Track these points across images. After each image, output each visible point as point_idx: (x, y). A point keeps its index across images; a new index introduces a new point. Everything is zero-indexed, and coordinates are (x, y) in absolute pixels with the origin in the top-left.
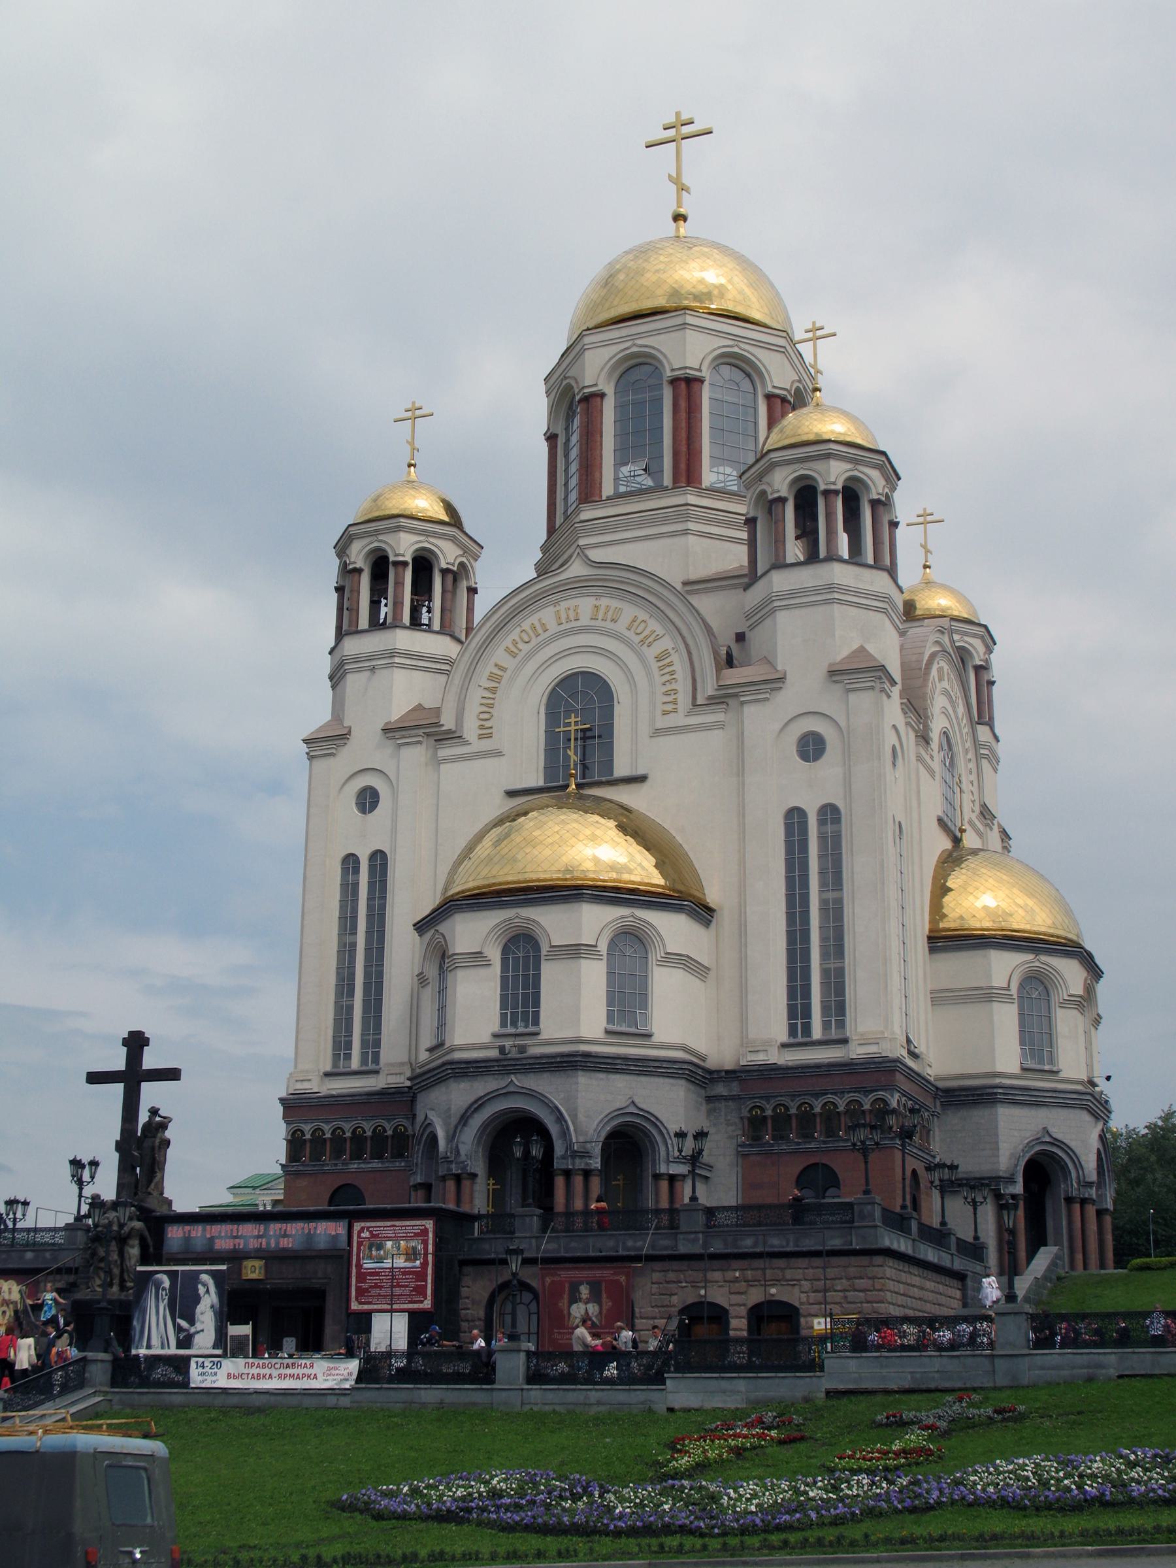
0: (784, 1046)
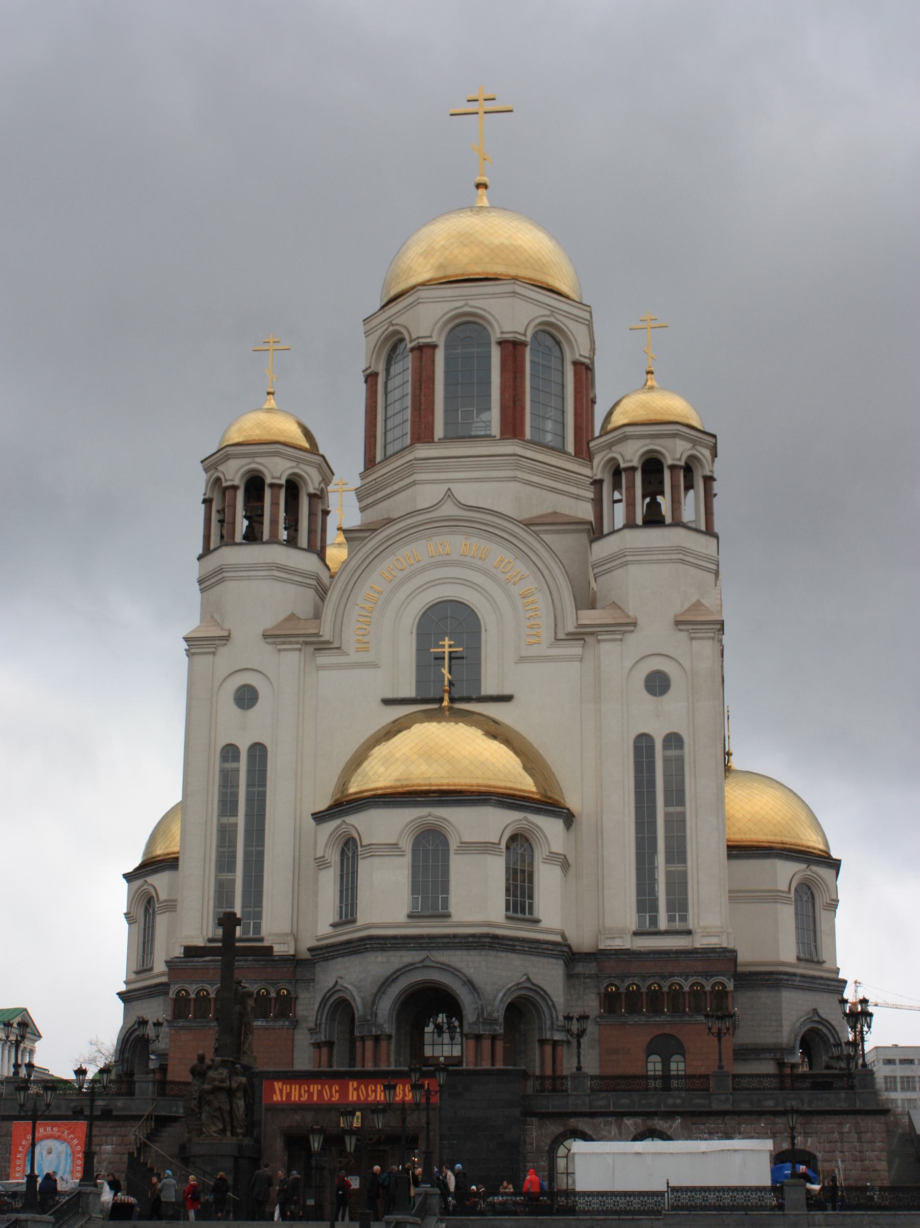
0: (635, 934)
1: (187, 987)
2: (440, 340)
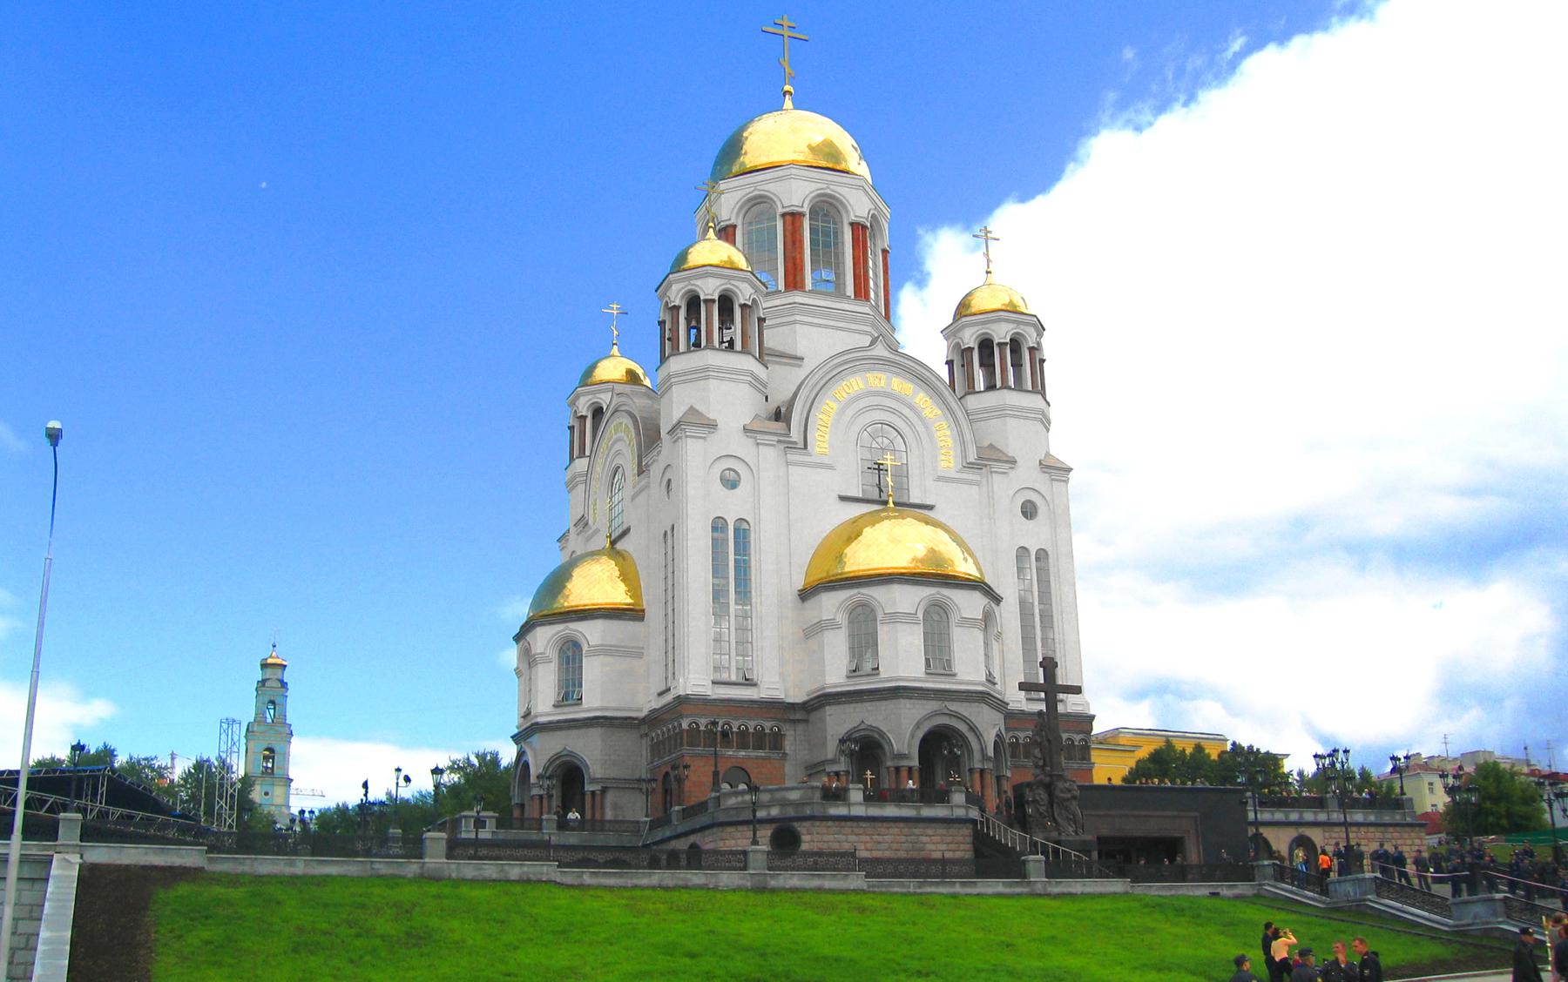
2: (806, 209)
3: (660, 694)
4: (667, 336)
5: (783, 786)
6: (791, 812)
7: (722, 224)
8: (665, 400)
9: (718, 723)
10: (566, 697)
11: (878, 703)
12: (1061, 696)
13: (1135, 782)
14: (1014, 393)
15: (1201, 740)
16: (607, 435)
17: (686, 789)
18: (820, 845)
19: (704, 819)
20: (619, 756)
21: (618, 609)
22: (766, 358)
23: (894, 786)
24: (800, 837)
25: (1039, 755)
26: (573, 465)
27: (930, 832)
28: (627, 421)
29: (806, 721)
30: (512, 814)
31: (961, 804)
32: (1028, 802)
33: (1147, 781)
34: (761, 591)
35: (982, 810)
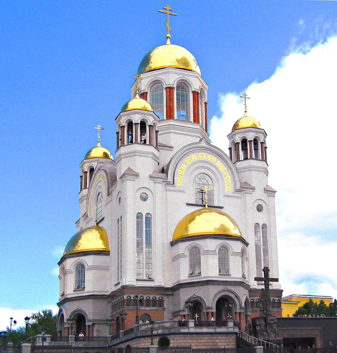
1: (130, 295)
3: (116, 285)
4: (119, 139)
5: (163, 321)
6: (166, 332)
7: (142, 92)
8: (118, 165)
9: (138, 296)
10: (78, 287)
11: (200, 287)
12: (270, 283)
13: (298, 316)
14: (255, 161)
15: (323, 299)
16: (95, 179)
17: (126, 323)
18: (178, 345)
19: (132, 335)
20: (99, 310)
21: (99, 251)
22: (159, 147)
23: (206, 320)
24: (170, 341)
25: (262, 306)
26: (82, 192)
27: (220, 338)
28: (103, 173)
29: (173, 295)
30: (57, 336)
31: (232, 326)
32: (257, 325)
33: (302, 315)
34: (155, 242)
35: (240, 329)
